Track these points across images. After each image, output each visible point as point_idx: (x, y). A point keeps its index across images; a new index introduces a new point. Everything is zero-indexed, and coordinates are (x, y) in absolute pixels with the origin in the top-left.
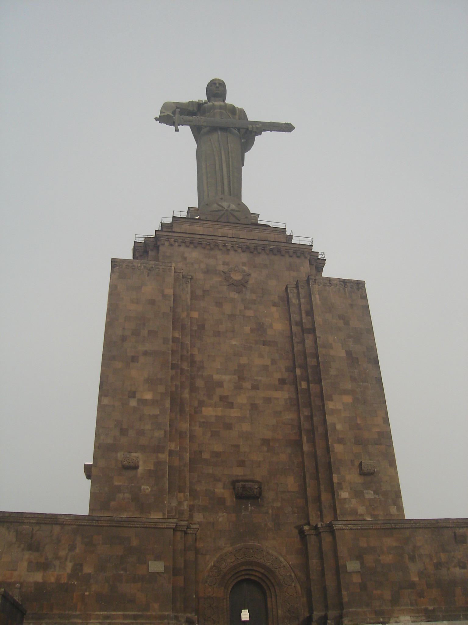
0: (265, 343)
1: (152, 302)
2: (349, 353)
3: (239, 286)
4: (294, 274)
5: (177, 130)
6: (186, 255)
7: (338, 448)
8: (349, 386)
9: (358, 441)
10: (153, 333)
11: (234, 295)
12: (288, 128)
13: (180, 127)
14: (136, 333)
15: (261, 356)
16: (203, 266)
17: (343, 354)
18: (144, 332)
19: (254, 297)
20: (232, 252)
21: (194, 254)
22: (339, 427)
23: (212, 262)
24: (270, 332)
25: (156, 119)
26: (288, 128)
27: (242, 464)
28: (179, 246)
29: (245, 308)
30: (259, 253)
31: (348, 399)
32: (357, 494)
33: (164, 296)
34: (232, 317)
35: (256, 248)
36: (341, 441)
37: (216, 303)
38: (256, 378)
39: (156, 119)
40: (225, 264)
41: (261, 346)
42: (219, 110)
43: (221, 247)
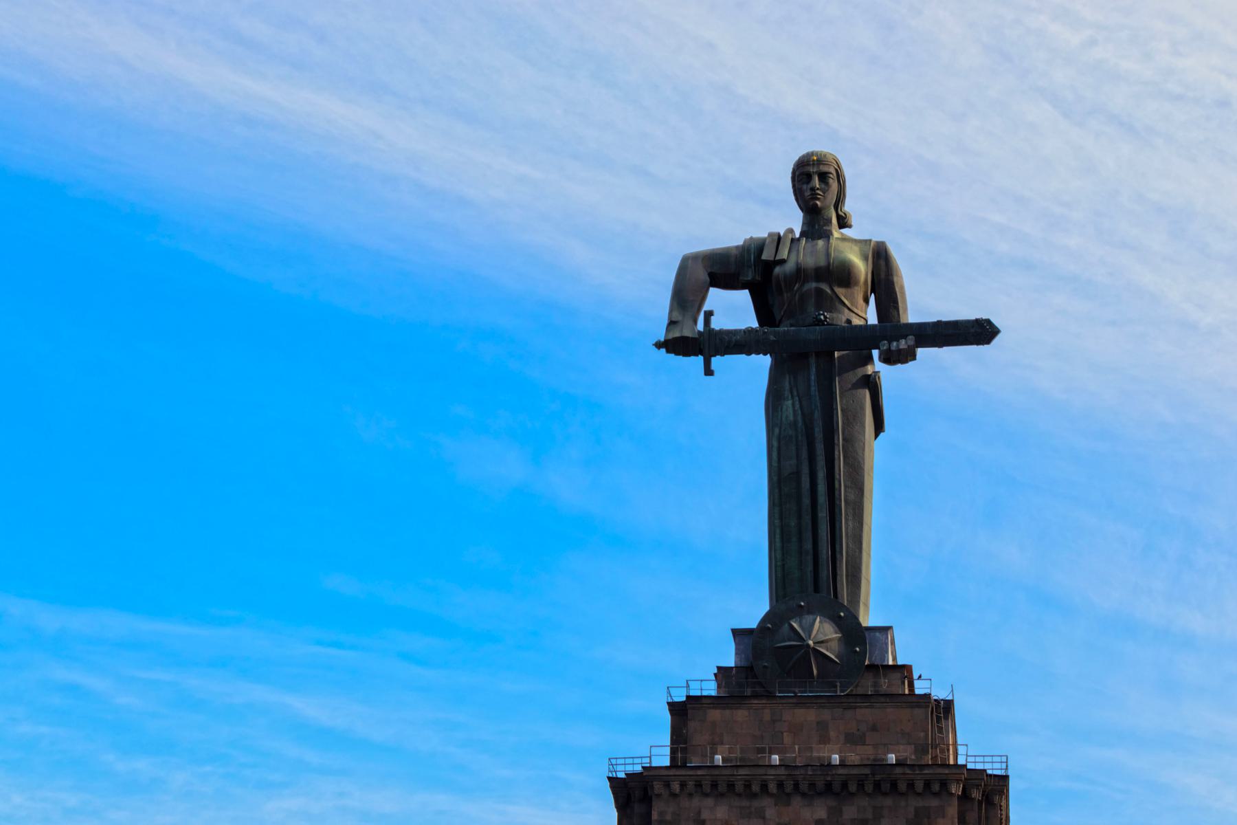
5: (709, 372)
6: (705, 815)
12: (979, 332)
13: (716, 361)
25: (659, 345)
26: (979, 332)
28: (690, 795)
30: (853, 794)
35: (845, 785)
39: (659, 345)
42: (814, 285)
43: (772, 787)
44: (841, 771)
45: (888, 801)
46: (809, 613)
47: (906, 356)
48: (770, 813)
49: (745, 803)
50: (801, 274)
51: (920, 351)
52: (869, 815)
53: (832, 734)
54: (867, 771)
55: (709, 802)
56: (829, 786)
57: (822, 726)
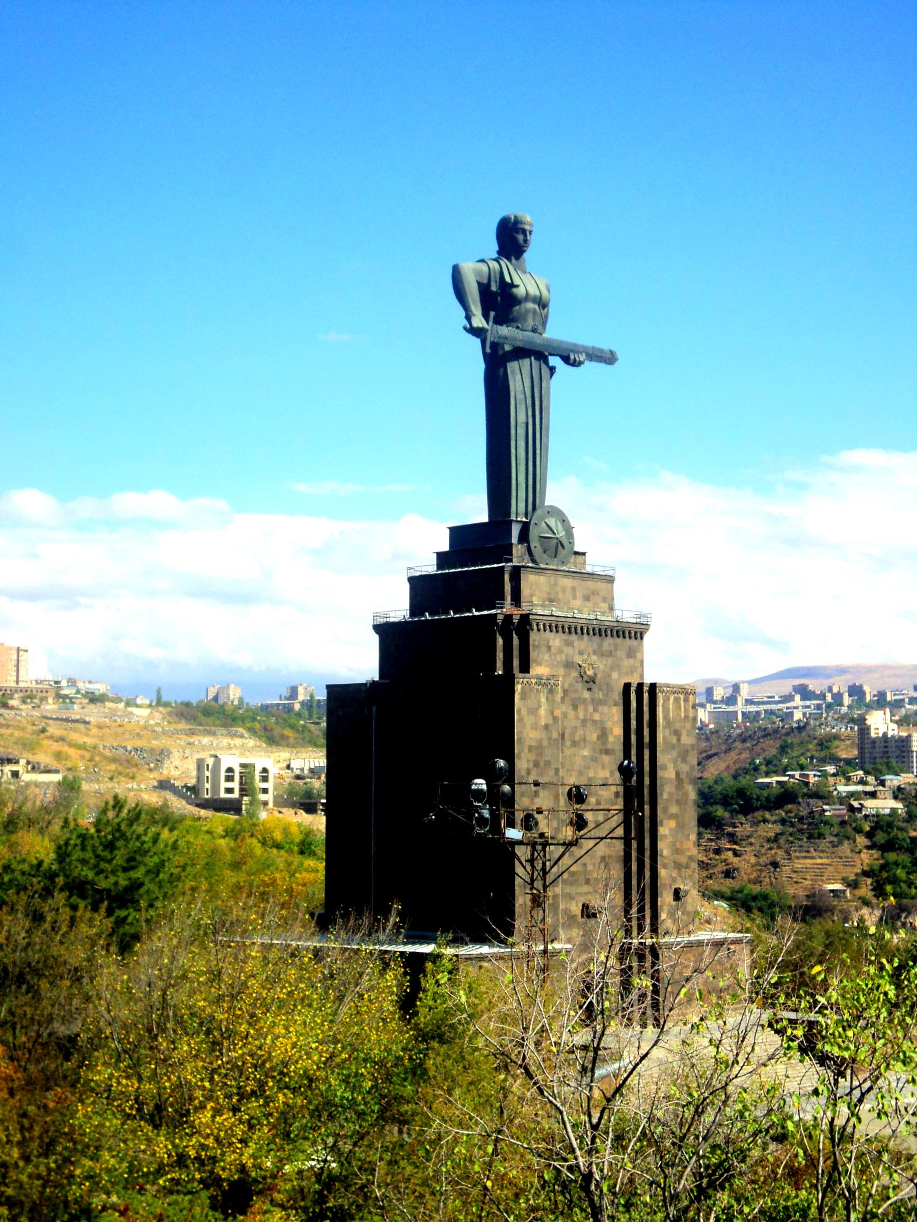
0: (607, 752)
1: (546, 727)
2: (677, 774)
3: (590, 682)
4: (631, 661)
6: (551, 644)
7: (662, 872)
8: (674, 809)
9: (678, 866)
10: (548, 763)
11: (586, 695)
14: (536, 764)
15: (603, 768)
16: (563, 656)
17: (673, 776)
18: (542, 764)
19: (601, 697)
20: (585, 636)
21: (556, 640)
22: (665, 853)
23: (568, 650)
24: (611, 739)
26: (609, 358)
27: (587, 882)
29: (594, 711)
31: (672, 824)
32: (672, 915)
33: (555, 719)
34: (584, 721)
36: (665, 866)
37: (573, 705)
38: (600, 792)
40: (581, 653)
41: (604, 756)
44: (606, 623)
45: (620, 640)
46: (552, 517)
47: (575, 364)
48: (576, 644)
49: (565, 637)
50: (527, 297)
51: (587, 362)
52: (612, 649)
53: (578, 594)
54: (615, 624)
55: (552, 635)
56: (600, 630)
57: (574, 589)
